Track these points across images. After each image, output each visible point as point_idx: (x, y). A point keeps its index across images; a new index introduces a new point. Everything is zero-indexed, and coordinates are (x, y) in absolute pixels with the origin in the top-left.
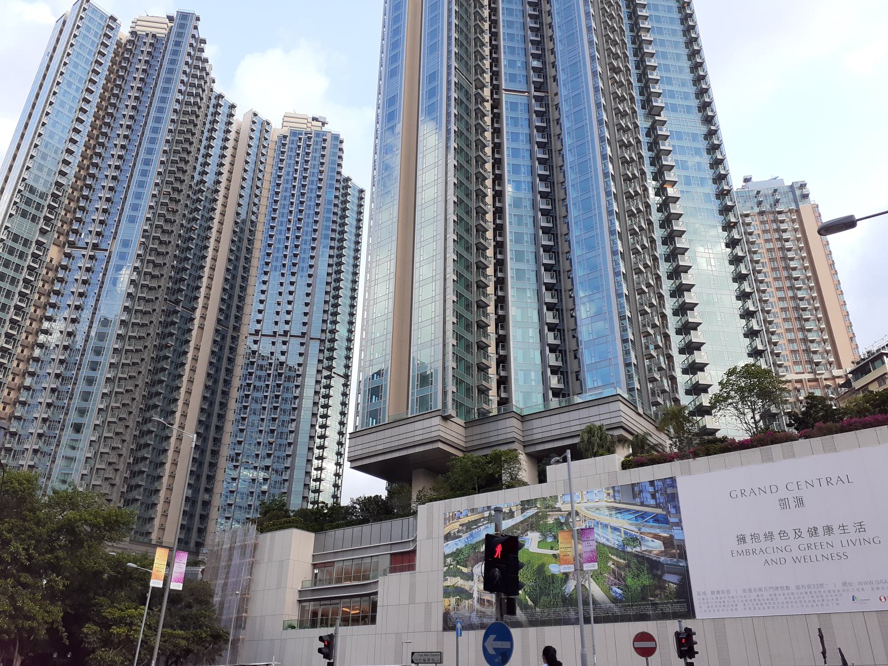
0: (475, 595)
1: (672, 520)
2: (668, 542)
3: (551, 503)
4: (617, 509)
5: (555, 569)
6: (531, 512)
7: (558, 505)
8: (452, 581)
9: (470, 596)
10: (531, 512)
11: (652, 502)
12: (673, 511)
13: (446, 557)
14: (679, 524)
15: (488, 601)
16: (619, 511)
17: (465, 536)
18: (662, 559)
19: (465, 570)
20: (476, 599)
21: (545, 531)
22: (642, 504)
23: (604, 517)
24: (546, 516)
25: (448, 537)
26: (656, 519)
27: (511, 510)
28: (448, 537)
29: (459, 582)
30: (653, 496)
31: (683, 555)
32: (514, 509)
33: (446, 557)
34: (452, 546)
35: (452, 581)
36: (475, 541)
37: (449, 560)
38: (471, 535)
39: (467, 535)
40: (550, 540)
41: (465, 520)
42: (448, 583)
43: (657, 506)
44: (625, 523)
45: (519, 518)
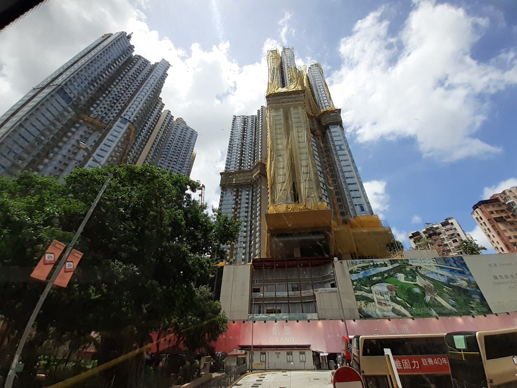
0: (375, 300)
1: (467, 273)
2: (469, 282)
3: (406, 262)
4: (439, 267)
5: (417, 290)
6: (396, 265)
7: (410, 263)
8: (359, 293)
9: (373, 301)
10: (396, 265)
11: (455, 265)
12: (466, 269)
13: (353, 281)
14: (471, 274)
15: (384, 304)
16: (441, 268)
17: (362, 273)
18: (468, 288)
19: (365, 288)
20: (376, 302)
21: (406, 274)
22: (451, 266)
23: (435, 270)
24: (405, 268)
25: (351, 272)
26: (460, 272)
27: (385, 263)
28: (351, 272)
29: (365, 294)
30: (455, 263)
31: (477, 287)
32: (386, 263)
33: (353, 281)
34: (355, 277)
35: (359, 293)
36: (368, 275)
37: (355, 283)
38: (366, 272)
39: (363, 272)
40: (410, 278)
41: (360, 265)
42: (356, 294)
43: (458, 267)
44: (446, 273)
45: (390, 267)
